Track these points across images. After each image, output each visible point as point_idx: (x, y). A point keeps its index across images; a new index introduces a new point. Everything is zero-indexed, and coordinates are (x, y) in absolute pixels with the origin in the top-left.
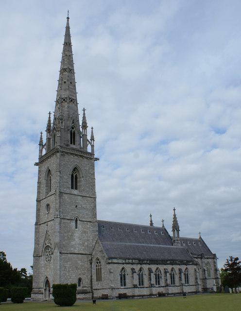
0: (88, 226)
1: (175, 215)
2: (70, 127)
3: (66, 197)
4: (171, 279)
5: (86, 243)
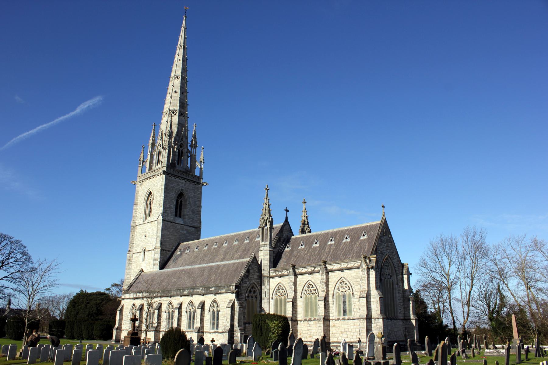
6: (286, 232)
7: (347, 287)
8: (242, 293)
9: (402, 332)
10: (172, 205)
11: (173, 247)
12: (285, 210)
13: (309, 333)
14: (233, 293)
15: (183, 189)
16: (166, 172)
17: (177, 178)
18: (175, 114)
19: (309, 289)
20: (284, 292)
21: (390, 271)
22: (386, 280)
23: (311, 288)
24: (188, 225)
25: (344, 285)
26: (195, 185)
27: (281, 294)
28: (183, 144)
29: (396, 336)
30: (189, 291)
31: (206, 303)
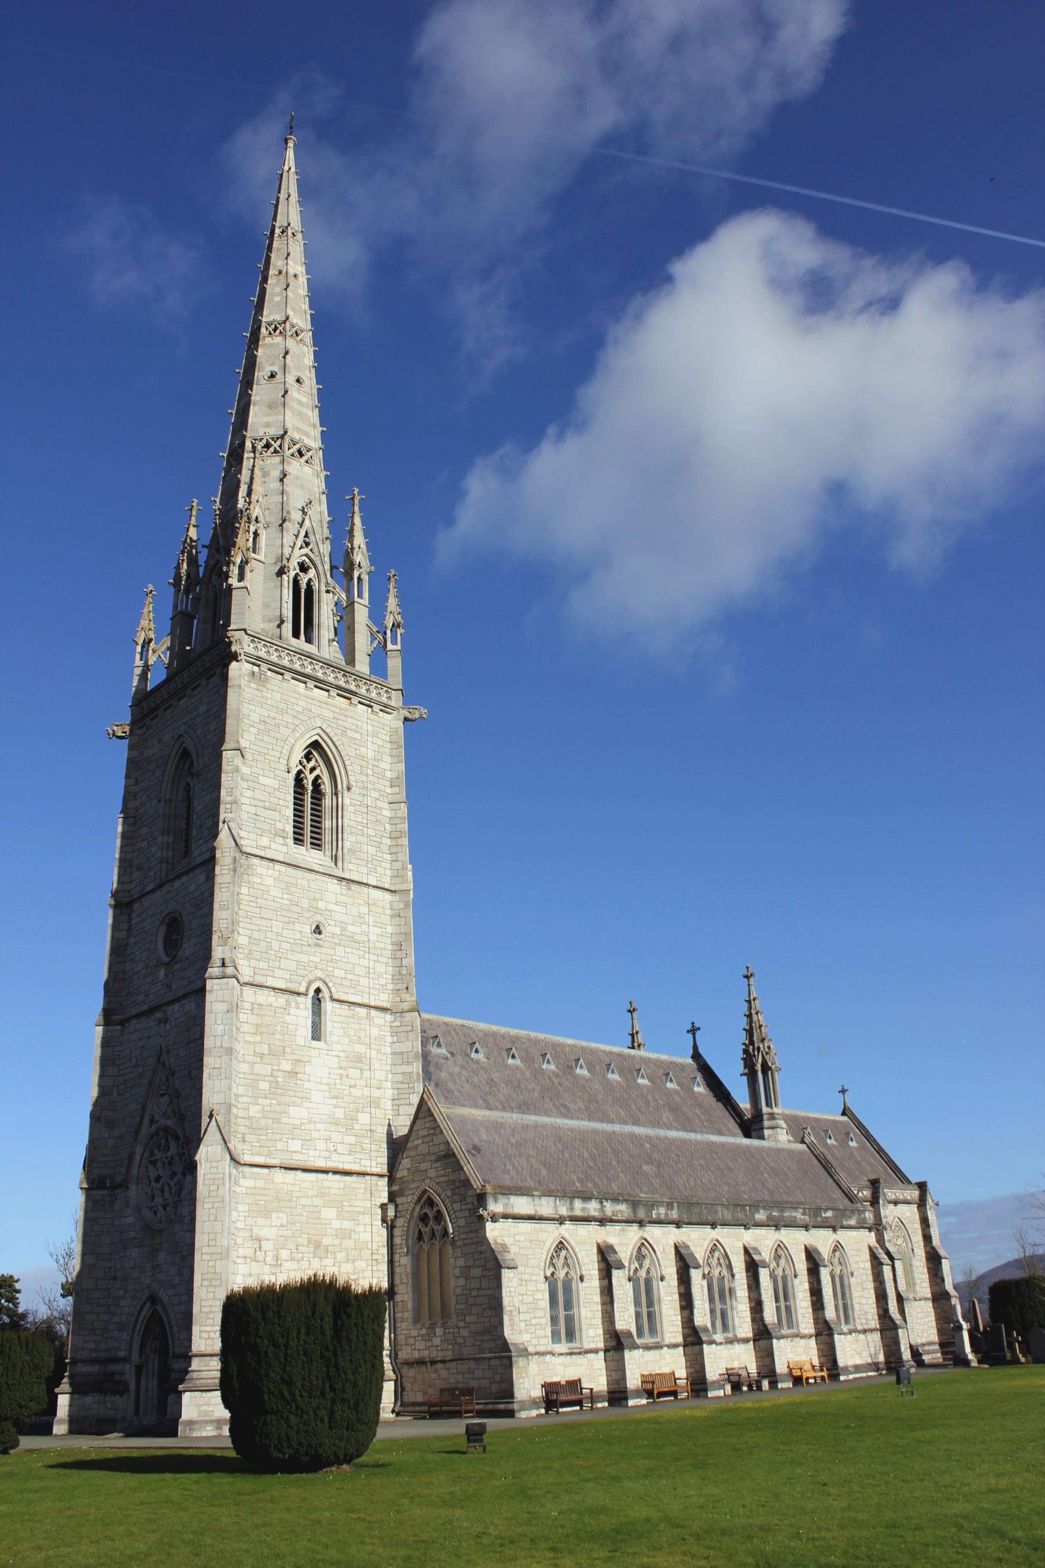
0: (375, 1032)
2: (294, 564)
4: (777, 1300)
5: (364, 1118)
30: (771, 1213)
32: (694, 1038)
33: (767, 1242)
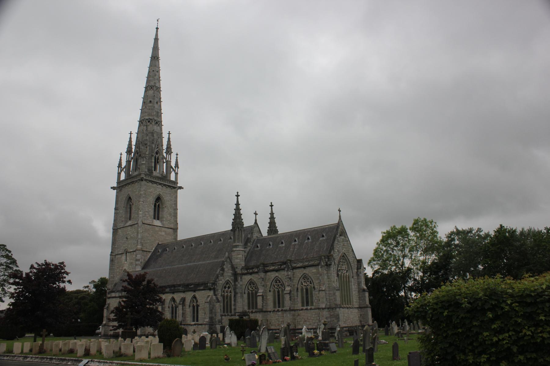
1: (238, 204)
3: (119, 231)
6: (255, 233)
7: (309, 281)
8: (218, 289)
9: (358, 319)
10: (150, 209)
11: (152, 248)
12: (254, 213)
13: (277, 322)
14: (210, 289)
15: (160, 194)
16: (144, 179)
17: (155, 184)
18: (151, 123)
19: (277, 284)
20: (255, 286)
21: (346, 266)
22: (342, 274)
23: (279, 284)
24: (166, 226)
25: (306, 280)
26: (171, 189)
27: (253, 289)
28: (159, 151)
29: (352, 322)
31: (186, 299)
32: (256, 216)
33: (169, 297)
